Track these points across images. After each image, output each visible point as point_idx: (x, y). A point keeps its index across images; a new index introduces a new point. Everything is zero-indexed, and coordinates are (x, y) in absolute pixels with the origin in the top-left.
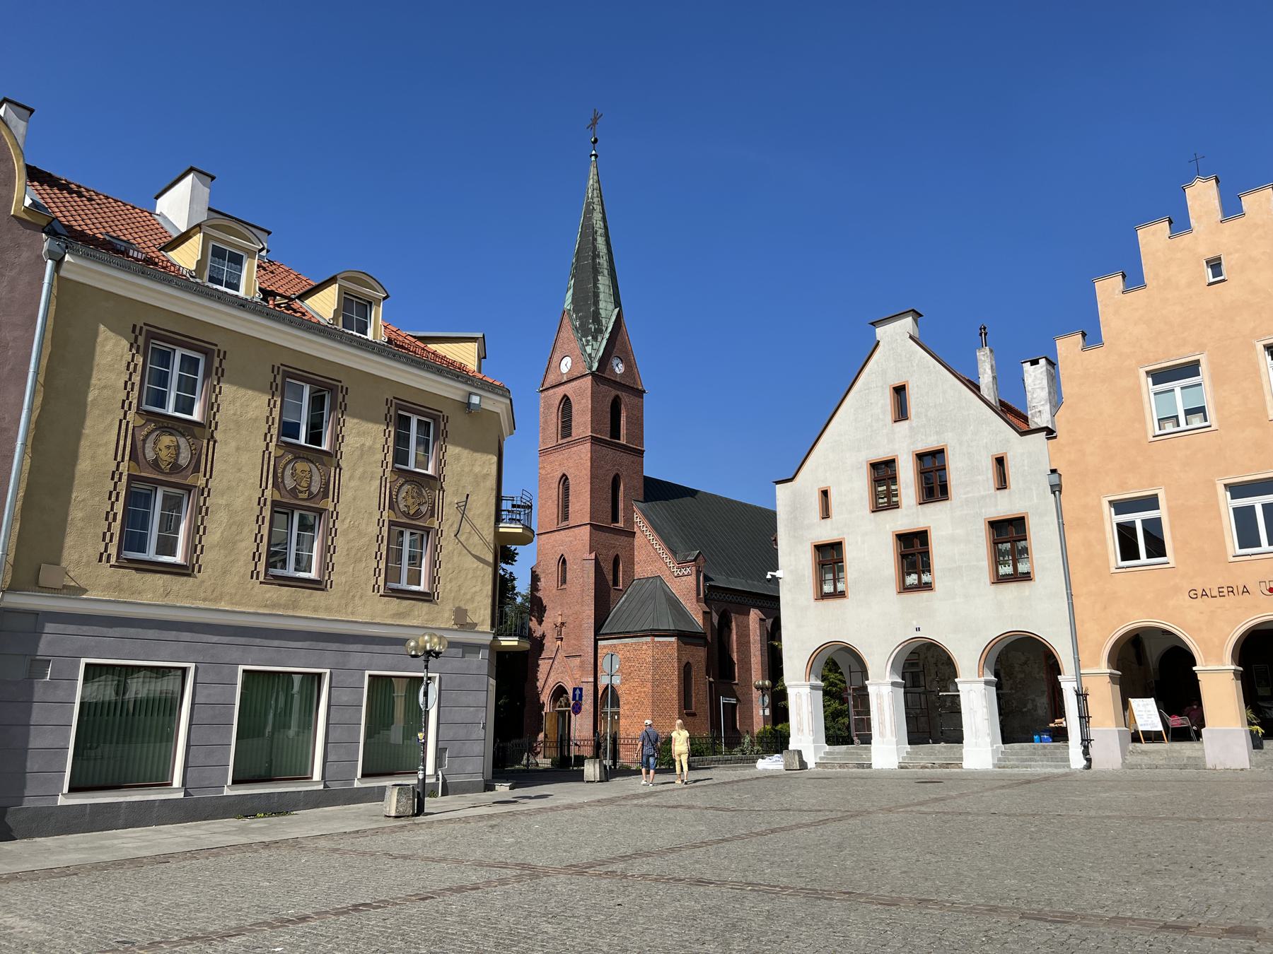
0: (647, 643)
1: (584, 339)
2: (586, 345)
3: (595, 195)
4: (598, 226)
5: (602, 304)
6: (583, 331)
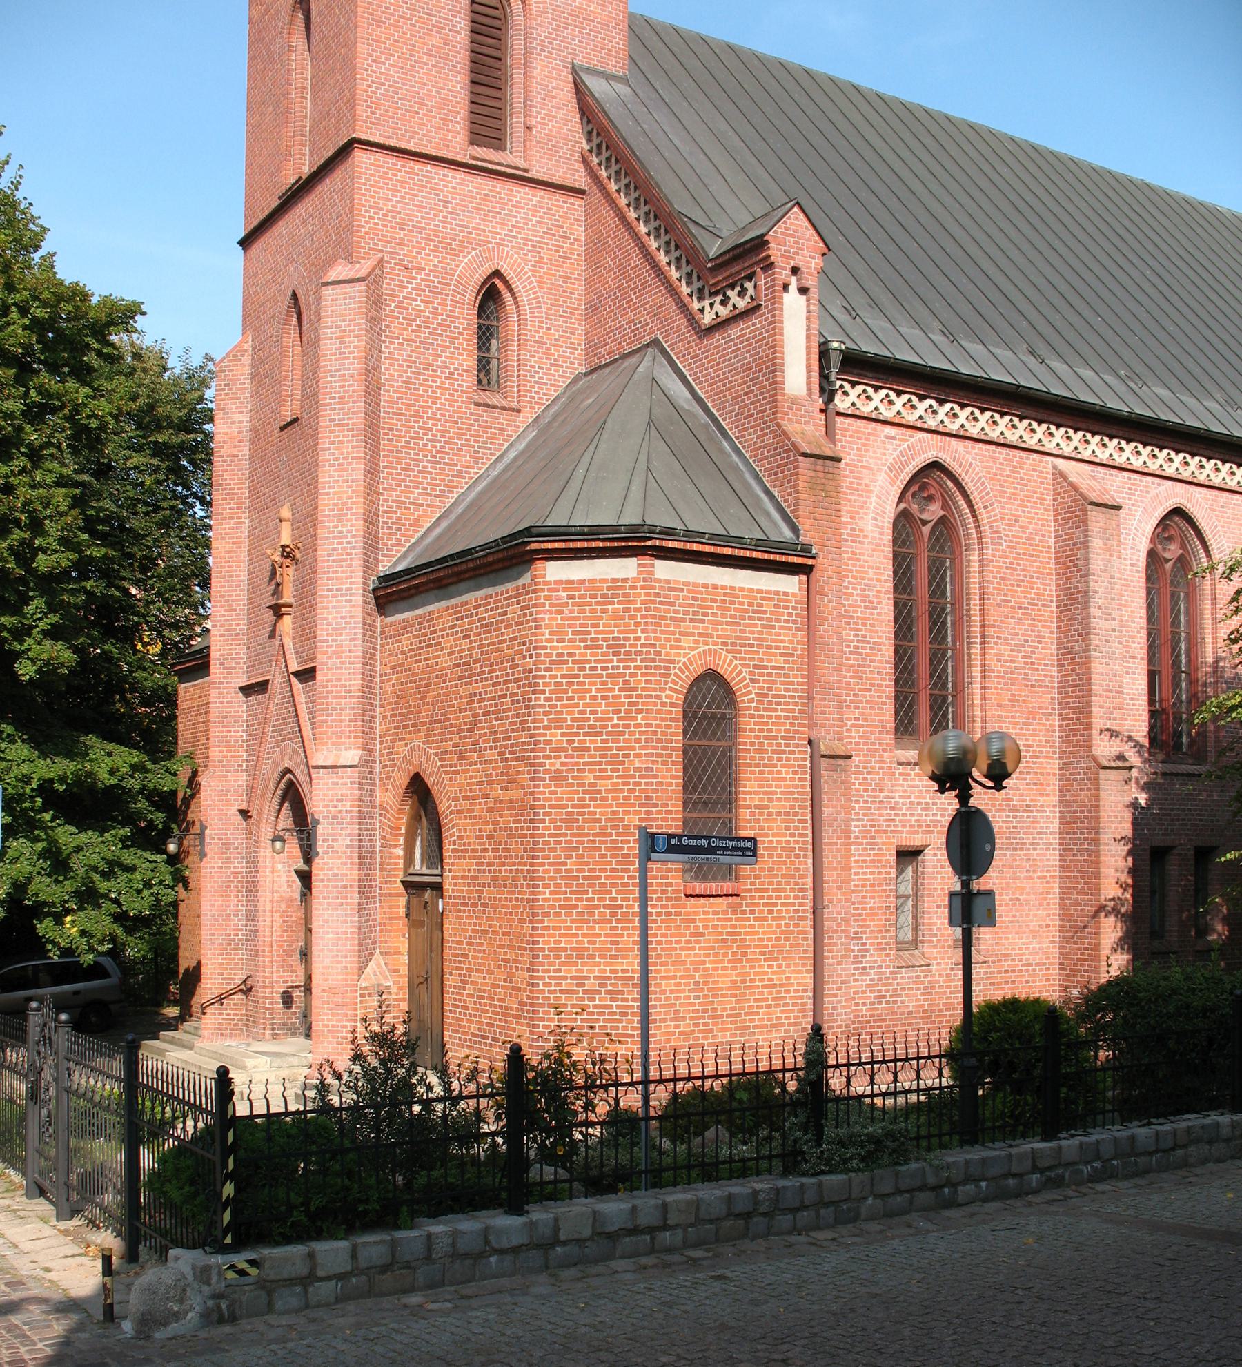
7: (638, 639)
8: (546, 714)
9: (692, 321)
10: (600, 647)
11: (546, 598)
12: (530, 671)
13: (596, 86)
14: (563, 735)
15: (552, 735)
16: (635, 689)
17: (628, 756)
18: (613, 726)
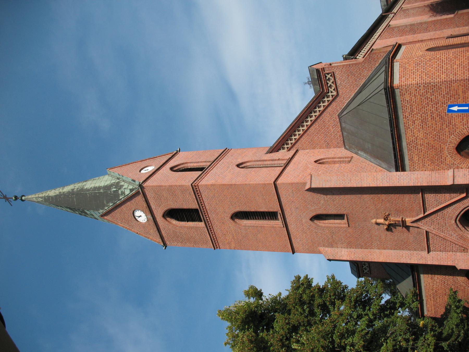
7: (416, 60)
8: (436, 79)
10: (418, 68)
11: (404, 83)
12: (424, 86)
14: (443, 74)
15: (443, 77)
16: (430, 59)
17: (449, 58)
18: (440, 62)
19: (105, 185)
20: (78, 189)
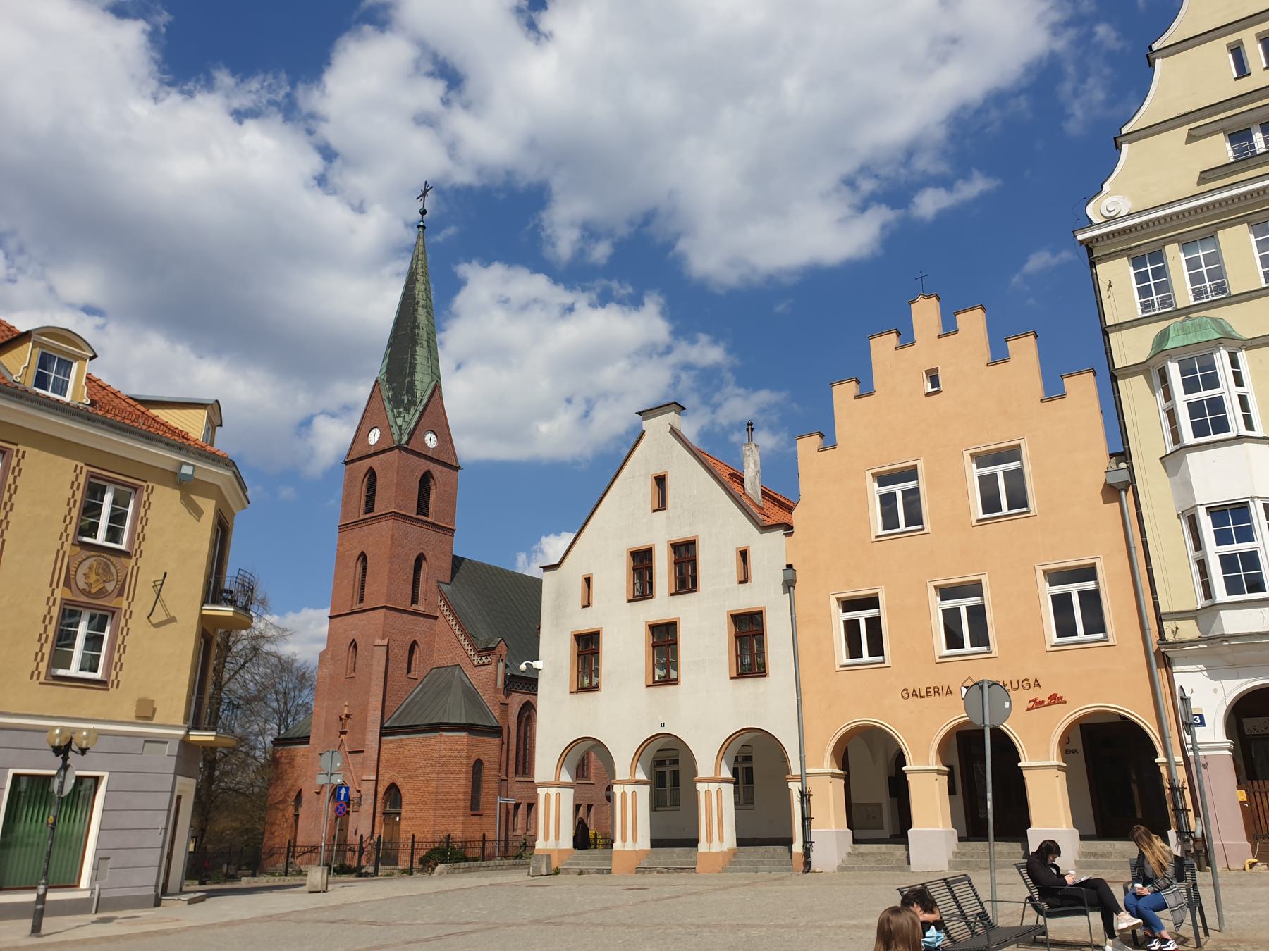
0: (435, 737)
1: (395, 411)
2: (397, 417)
3: (420, 266)
4: (420, 296)
5: (418, 376)
6: (396, 402)
9: (472, 662)
13: (444, 587)
19: (416, 382)
20: (418, 334)
